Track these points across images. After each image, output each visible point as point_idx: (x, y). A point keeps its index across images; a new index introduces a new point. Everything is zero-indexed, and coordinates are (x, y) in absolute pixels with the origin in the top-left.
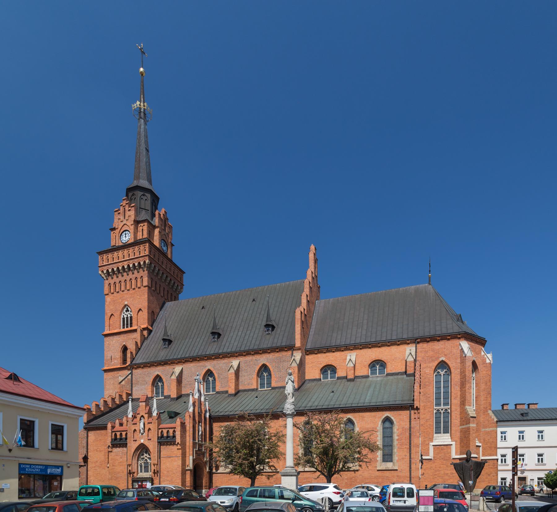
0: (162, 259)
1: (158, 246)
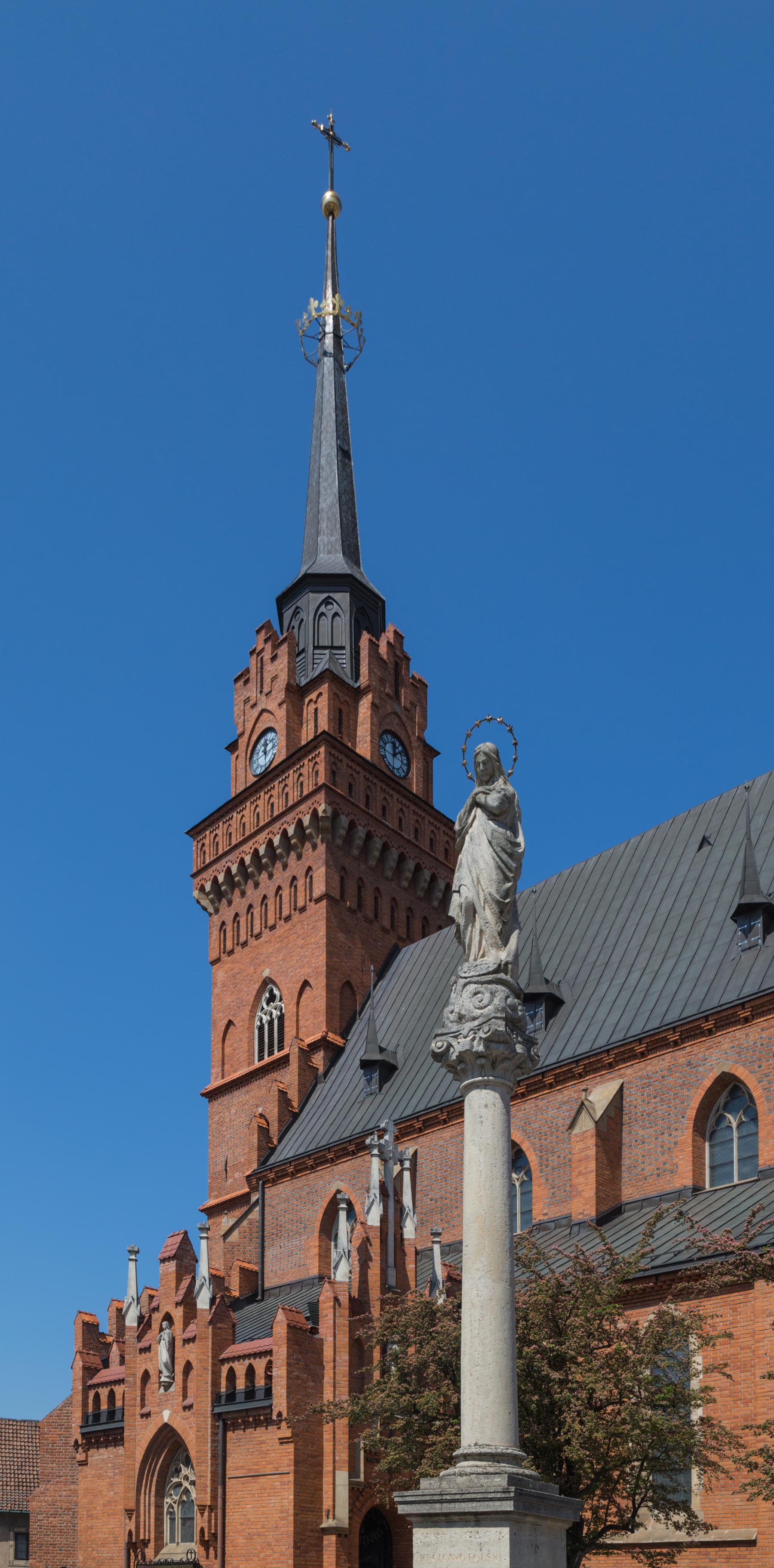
0: (380, 796)
1: (368, 757)
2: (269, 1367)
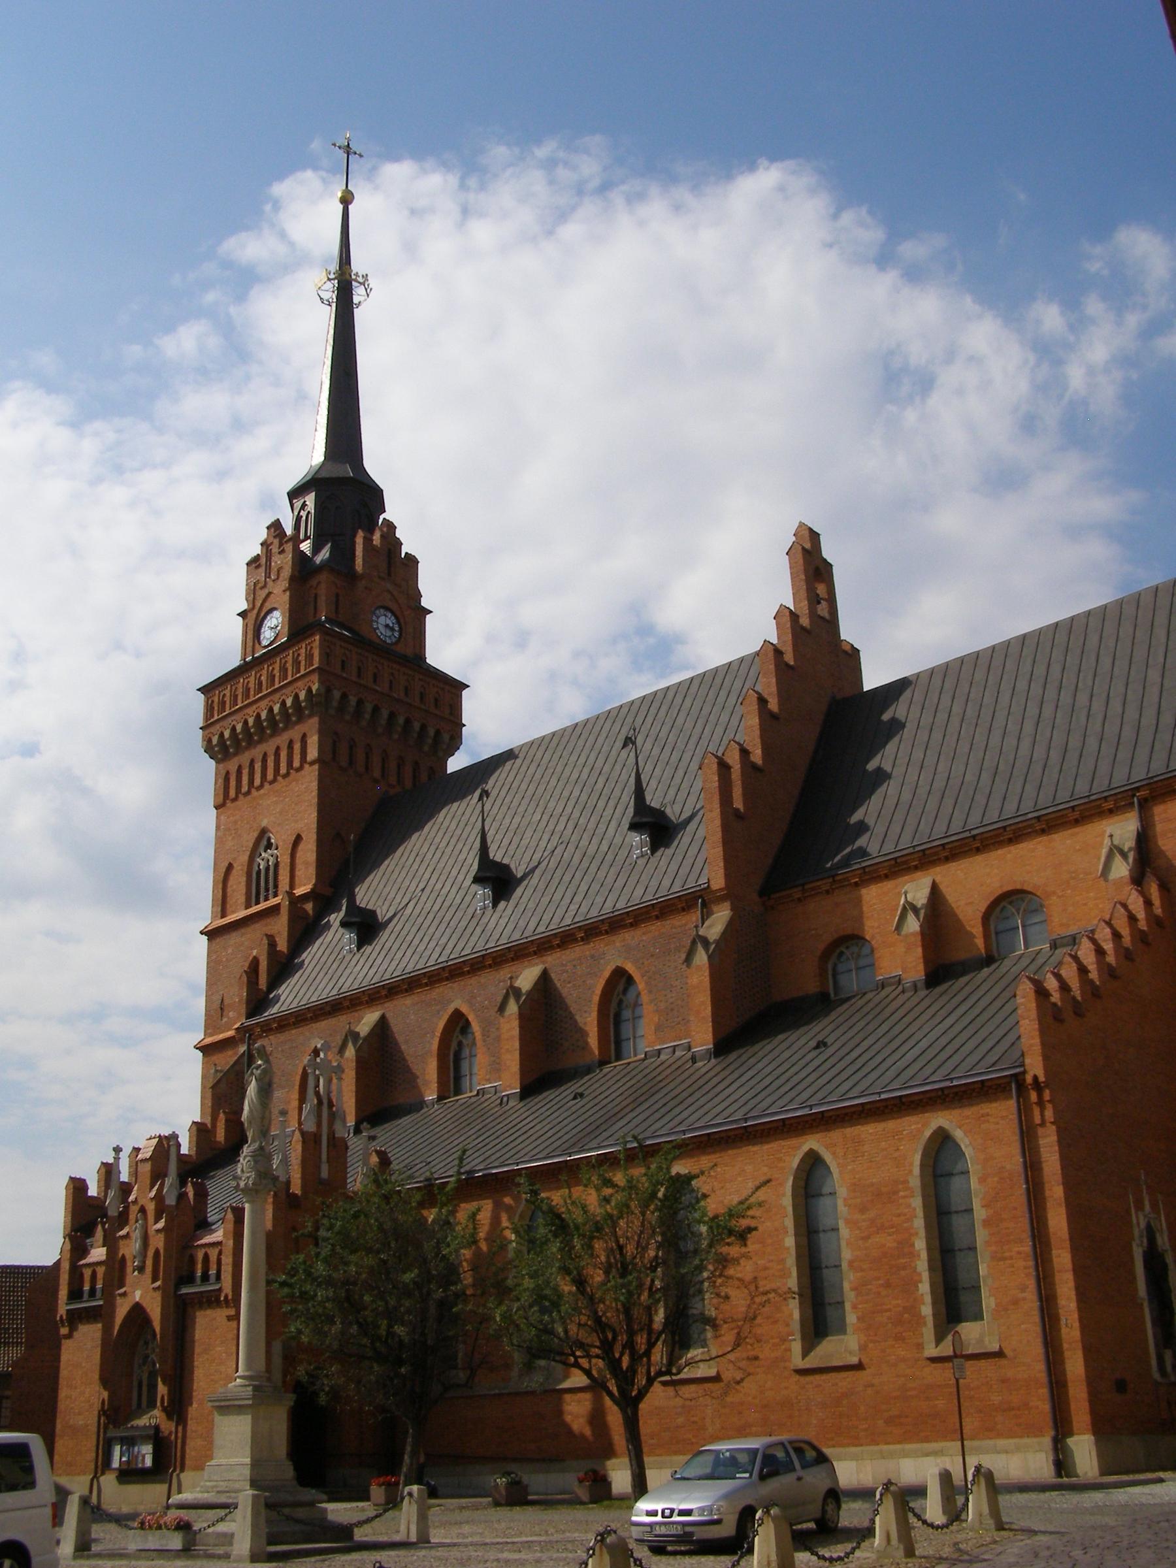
2: (220, 1253)
